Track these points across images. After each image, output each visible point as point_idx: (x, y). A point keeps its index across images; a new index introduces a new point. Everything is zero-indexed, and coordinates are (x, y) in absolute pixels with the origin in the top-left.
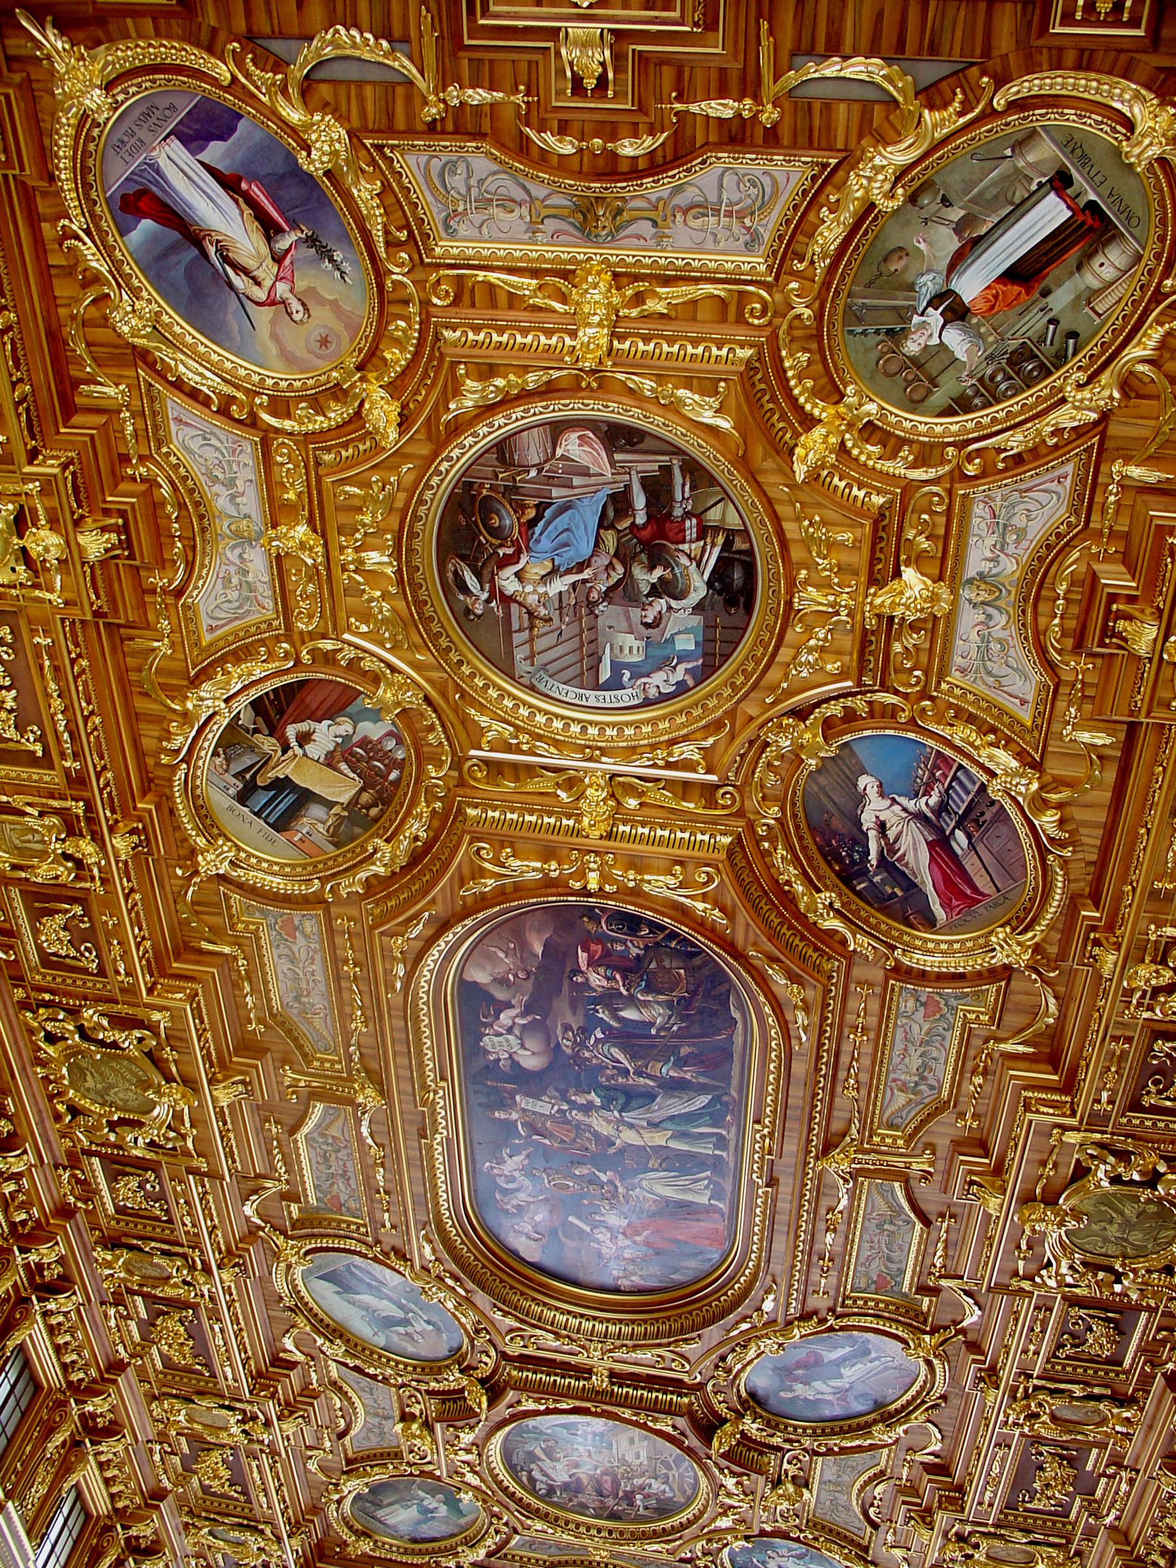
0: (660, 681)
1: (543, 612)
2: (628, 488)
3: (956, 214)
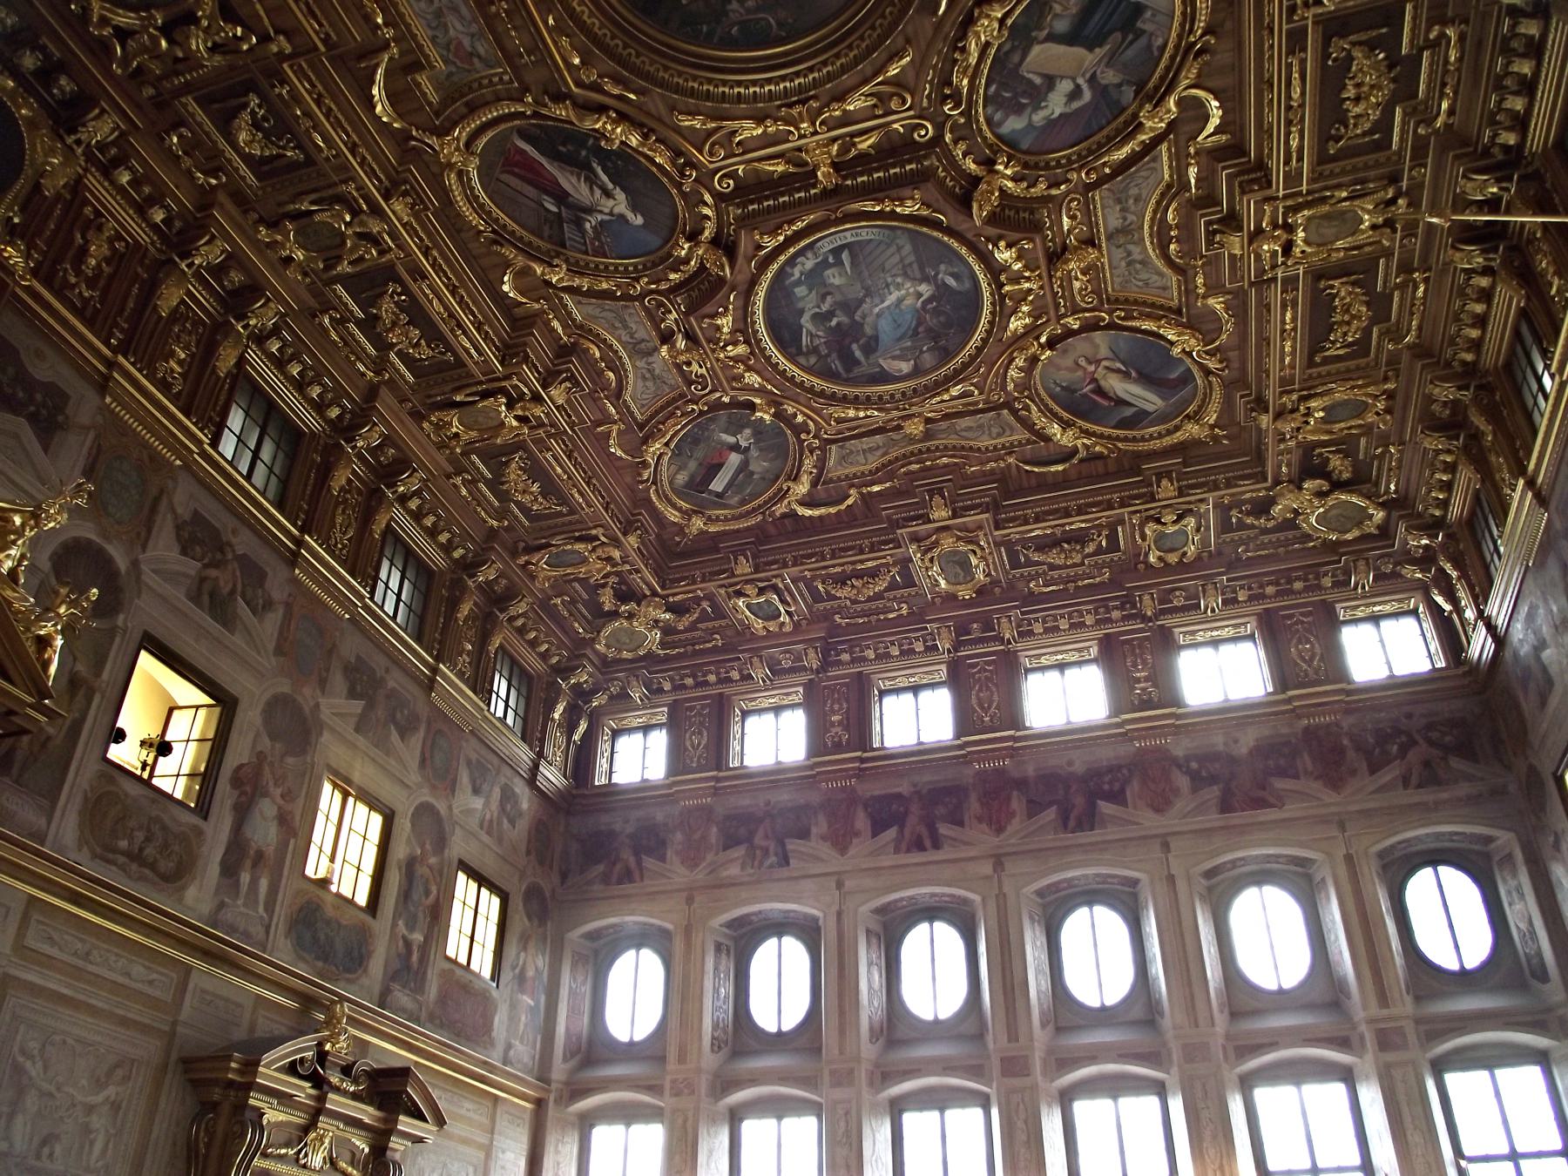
0: (809, 263)
1: (899, 280)
2: (867, 358)
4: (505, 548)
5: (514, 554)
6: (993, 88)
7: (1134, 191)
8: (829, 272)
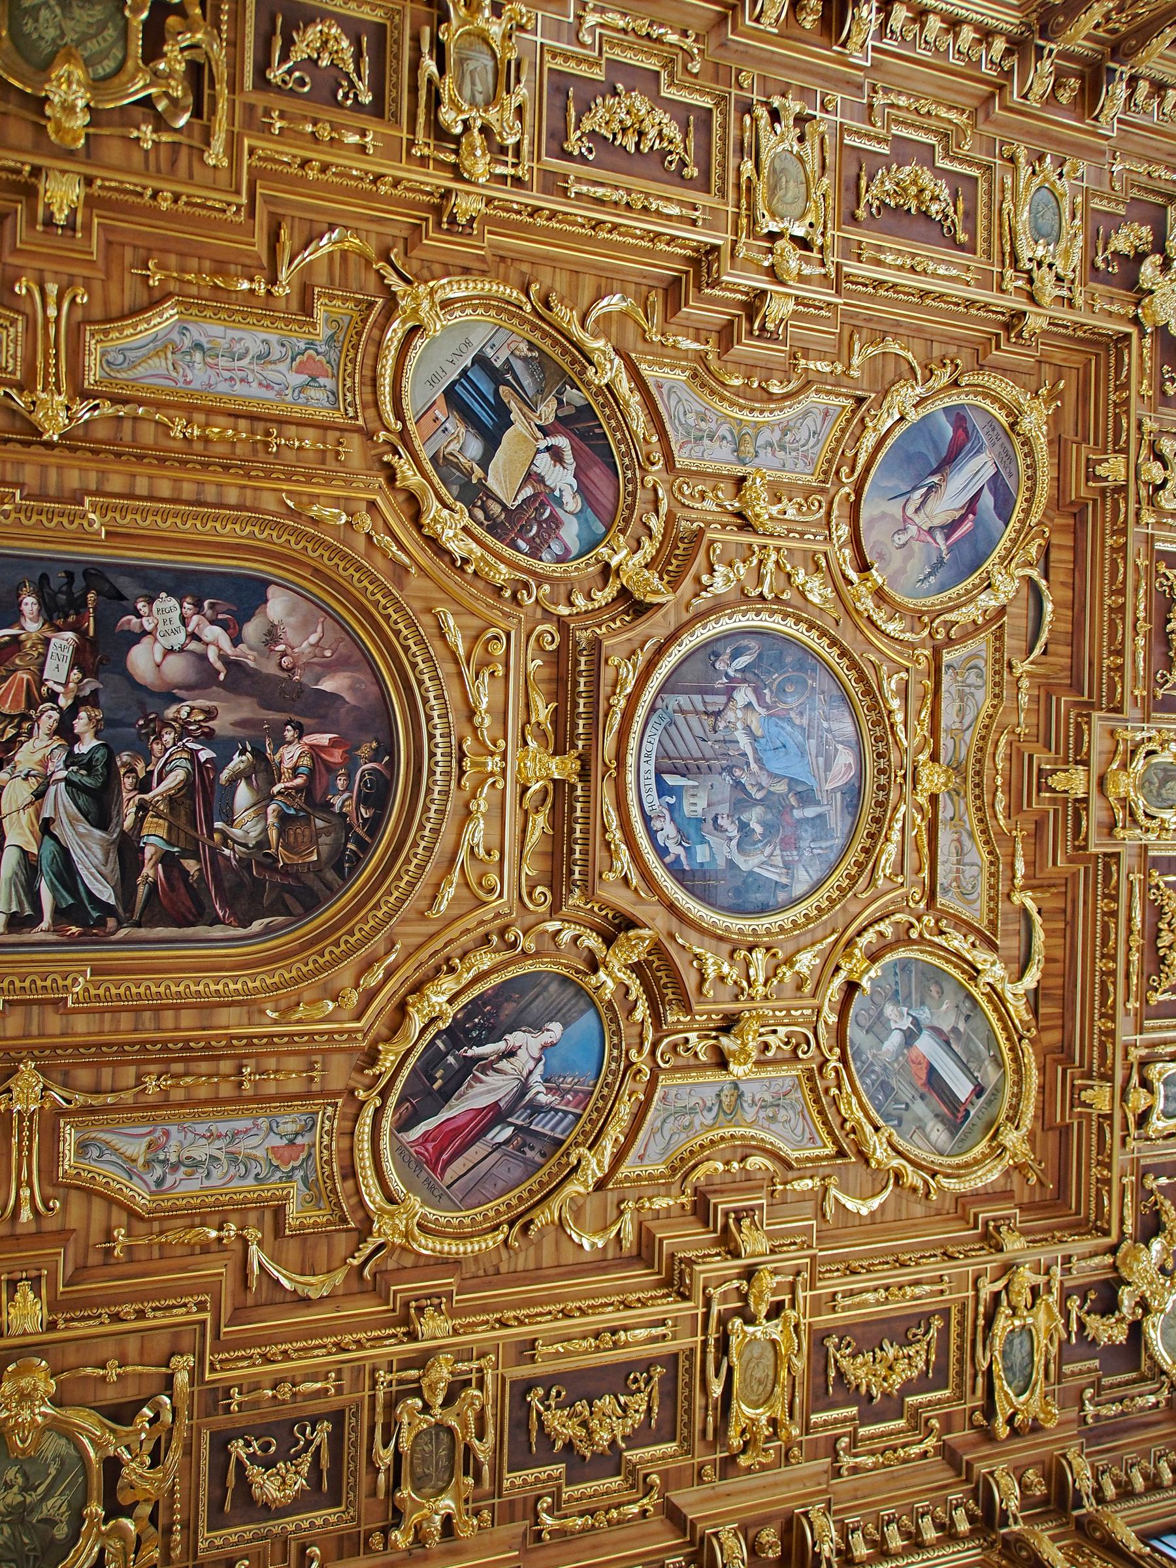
0: (667, 831)
1: (721, 725)
3: (961, 1026)
4: (975, 1445)
5: (988, 1436)
6: (522, 544)
7: (691, 419)
8: (687, 809)
